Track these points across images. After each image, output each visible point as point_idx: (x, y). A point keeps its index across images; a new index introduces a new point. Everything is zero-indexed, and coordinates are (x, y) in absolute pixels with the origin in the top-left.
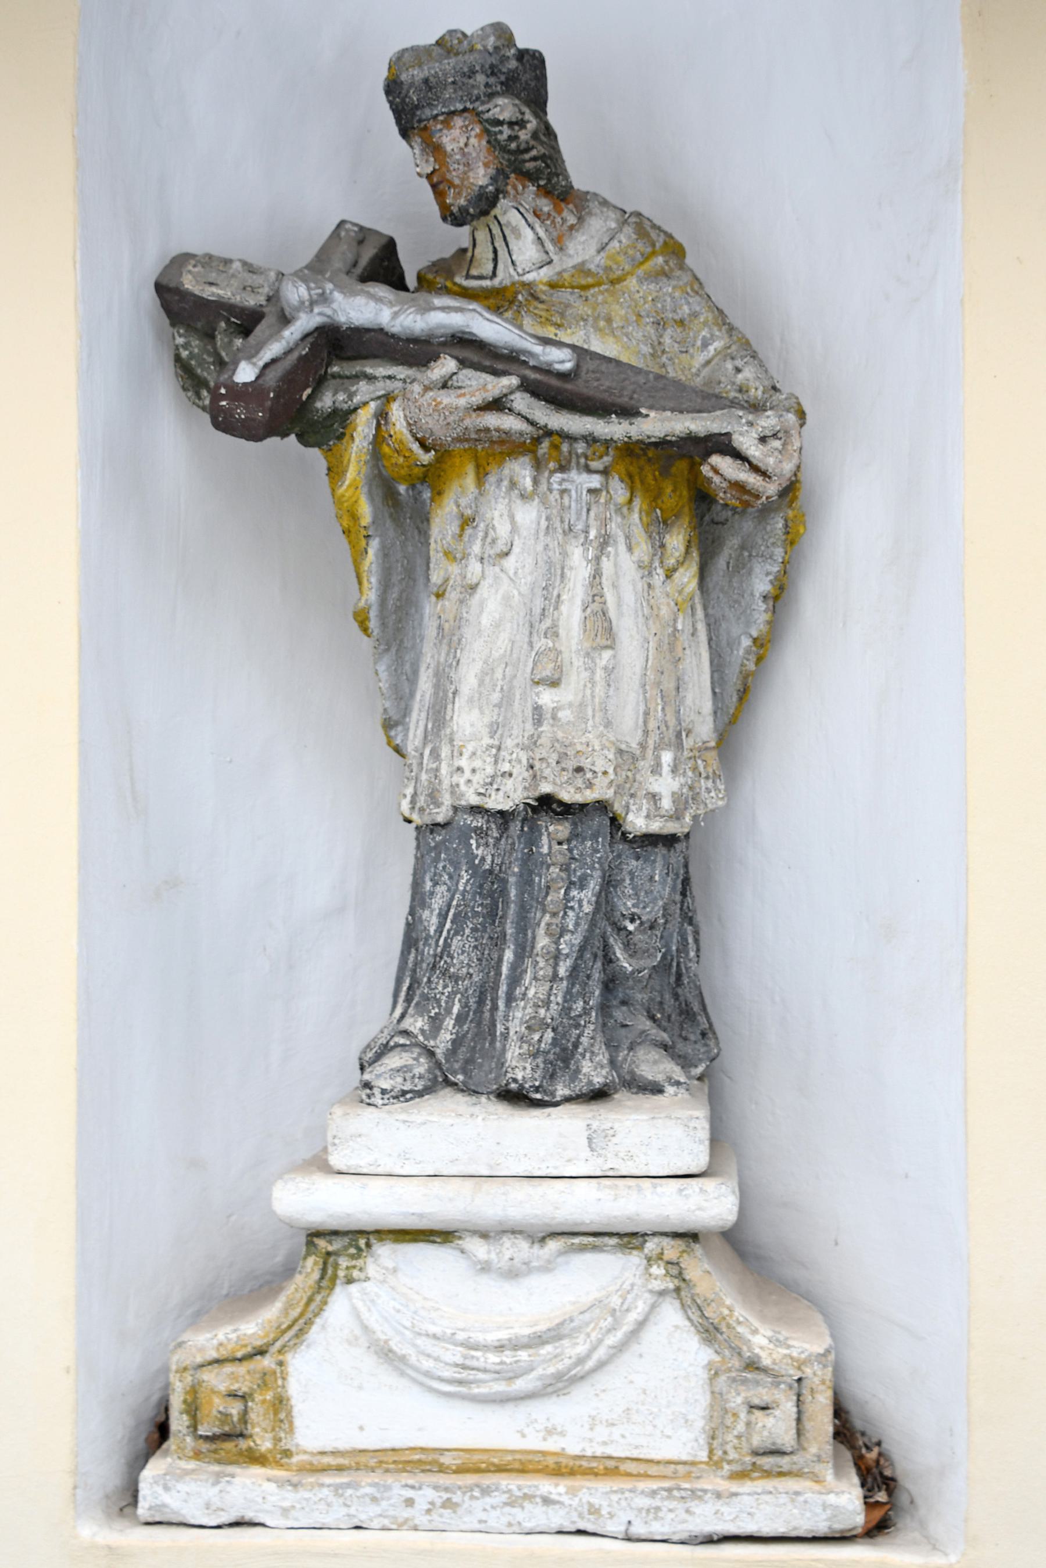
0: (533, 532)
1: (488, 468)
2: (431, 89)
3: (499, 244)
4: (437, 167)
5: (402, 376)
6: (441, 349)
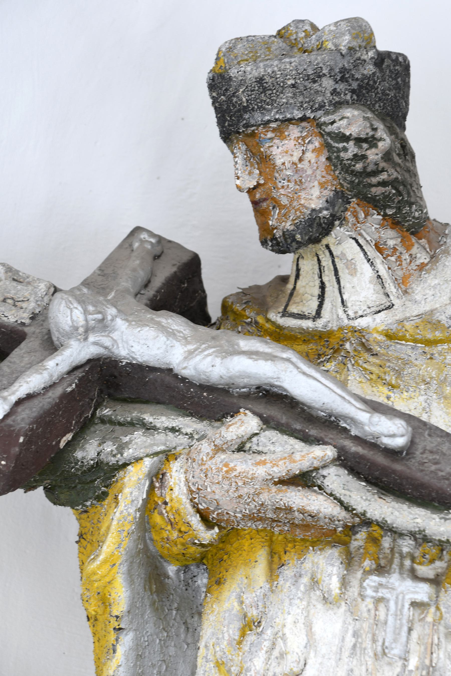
0: (334, 649)
1: (285, 558)
2: (265, 90)
3: (329, 278)
4: (262, 182)
5: (189, 430)
6: (242, 402)
